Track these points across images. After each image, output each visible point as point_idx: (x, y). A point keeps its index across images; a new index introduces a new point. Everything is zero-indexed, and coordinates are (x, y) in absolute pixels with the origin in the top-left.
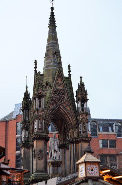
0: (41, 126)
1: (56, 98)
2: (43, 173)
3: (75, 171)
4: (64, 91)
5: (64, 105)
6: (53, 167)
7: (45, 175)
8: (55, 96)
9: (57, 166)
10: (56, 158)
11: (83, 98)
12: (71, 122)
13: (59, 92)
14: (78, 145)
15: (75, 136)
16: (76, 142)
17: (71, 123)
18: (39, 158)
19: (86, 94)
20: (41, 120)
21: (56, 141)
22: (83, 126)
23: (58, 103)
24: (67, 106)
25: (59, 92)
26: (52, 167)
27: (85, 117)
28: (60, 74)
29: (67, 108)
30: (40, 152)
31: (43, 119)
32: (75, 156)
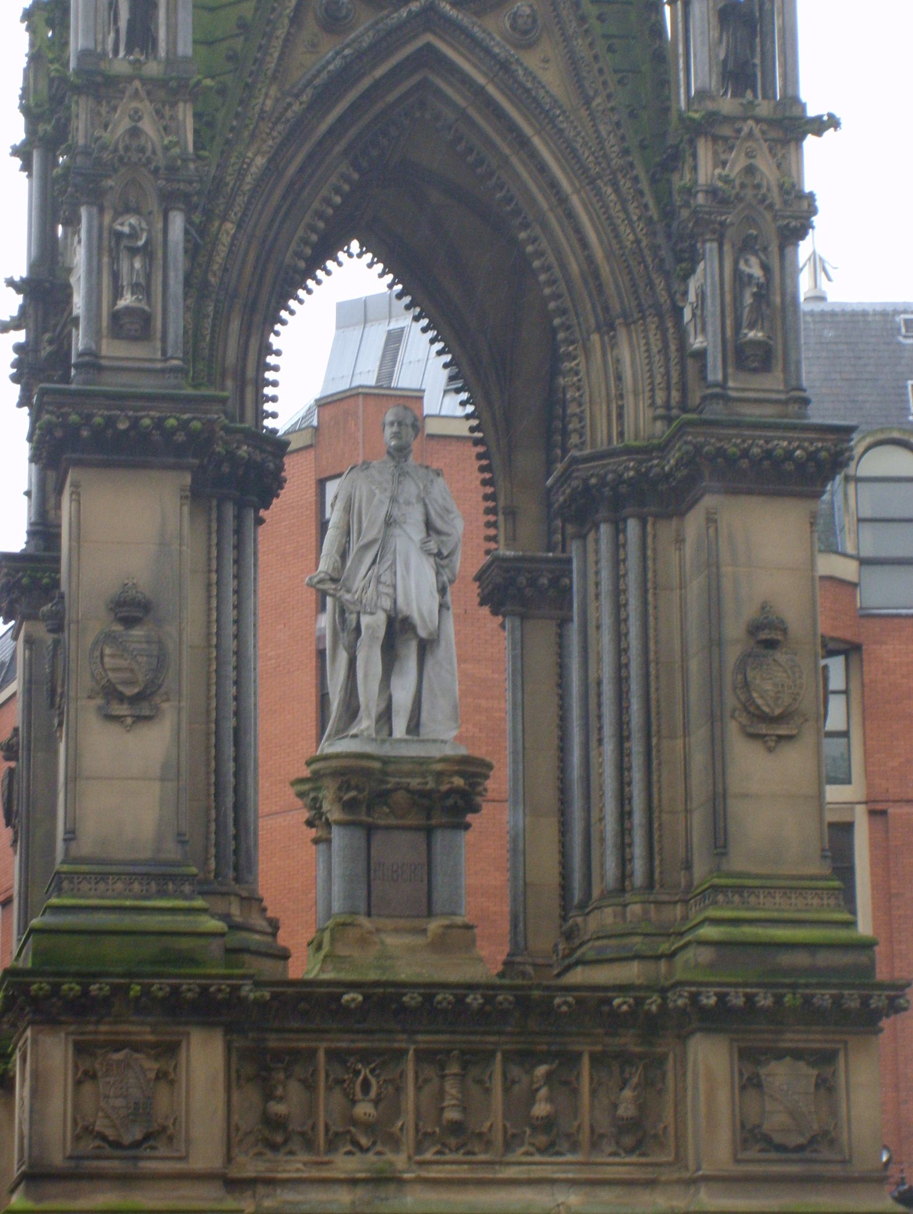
0: (143, 288)
2: (162, 894)
3: (639, 878)
6: (370, 830)
7: (181, 922)
10: (414, 726)
12: (584, 244)
14: (680, 541)
15: (641, 421)
16: (655, 490)
17: (590, 260)
18: (111, 693)
20: (153, 204)
21: (416, 515)
24: (525, 35)
26: (359, 835)
29: (531, 60)
30: (129, 622)
31: (169, 200)
32: (635, 686)
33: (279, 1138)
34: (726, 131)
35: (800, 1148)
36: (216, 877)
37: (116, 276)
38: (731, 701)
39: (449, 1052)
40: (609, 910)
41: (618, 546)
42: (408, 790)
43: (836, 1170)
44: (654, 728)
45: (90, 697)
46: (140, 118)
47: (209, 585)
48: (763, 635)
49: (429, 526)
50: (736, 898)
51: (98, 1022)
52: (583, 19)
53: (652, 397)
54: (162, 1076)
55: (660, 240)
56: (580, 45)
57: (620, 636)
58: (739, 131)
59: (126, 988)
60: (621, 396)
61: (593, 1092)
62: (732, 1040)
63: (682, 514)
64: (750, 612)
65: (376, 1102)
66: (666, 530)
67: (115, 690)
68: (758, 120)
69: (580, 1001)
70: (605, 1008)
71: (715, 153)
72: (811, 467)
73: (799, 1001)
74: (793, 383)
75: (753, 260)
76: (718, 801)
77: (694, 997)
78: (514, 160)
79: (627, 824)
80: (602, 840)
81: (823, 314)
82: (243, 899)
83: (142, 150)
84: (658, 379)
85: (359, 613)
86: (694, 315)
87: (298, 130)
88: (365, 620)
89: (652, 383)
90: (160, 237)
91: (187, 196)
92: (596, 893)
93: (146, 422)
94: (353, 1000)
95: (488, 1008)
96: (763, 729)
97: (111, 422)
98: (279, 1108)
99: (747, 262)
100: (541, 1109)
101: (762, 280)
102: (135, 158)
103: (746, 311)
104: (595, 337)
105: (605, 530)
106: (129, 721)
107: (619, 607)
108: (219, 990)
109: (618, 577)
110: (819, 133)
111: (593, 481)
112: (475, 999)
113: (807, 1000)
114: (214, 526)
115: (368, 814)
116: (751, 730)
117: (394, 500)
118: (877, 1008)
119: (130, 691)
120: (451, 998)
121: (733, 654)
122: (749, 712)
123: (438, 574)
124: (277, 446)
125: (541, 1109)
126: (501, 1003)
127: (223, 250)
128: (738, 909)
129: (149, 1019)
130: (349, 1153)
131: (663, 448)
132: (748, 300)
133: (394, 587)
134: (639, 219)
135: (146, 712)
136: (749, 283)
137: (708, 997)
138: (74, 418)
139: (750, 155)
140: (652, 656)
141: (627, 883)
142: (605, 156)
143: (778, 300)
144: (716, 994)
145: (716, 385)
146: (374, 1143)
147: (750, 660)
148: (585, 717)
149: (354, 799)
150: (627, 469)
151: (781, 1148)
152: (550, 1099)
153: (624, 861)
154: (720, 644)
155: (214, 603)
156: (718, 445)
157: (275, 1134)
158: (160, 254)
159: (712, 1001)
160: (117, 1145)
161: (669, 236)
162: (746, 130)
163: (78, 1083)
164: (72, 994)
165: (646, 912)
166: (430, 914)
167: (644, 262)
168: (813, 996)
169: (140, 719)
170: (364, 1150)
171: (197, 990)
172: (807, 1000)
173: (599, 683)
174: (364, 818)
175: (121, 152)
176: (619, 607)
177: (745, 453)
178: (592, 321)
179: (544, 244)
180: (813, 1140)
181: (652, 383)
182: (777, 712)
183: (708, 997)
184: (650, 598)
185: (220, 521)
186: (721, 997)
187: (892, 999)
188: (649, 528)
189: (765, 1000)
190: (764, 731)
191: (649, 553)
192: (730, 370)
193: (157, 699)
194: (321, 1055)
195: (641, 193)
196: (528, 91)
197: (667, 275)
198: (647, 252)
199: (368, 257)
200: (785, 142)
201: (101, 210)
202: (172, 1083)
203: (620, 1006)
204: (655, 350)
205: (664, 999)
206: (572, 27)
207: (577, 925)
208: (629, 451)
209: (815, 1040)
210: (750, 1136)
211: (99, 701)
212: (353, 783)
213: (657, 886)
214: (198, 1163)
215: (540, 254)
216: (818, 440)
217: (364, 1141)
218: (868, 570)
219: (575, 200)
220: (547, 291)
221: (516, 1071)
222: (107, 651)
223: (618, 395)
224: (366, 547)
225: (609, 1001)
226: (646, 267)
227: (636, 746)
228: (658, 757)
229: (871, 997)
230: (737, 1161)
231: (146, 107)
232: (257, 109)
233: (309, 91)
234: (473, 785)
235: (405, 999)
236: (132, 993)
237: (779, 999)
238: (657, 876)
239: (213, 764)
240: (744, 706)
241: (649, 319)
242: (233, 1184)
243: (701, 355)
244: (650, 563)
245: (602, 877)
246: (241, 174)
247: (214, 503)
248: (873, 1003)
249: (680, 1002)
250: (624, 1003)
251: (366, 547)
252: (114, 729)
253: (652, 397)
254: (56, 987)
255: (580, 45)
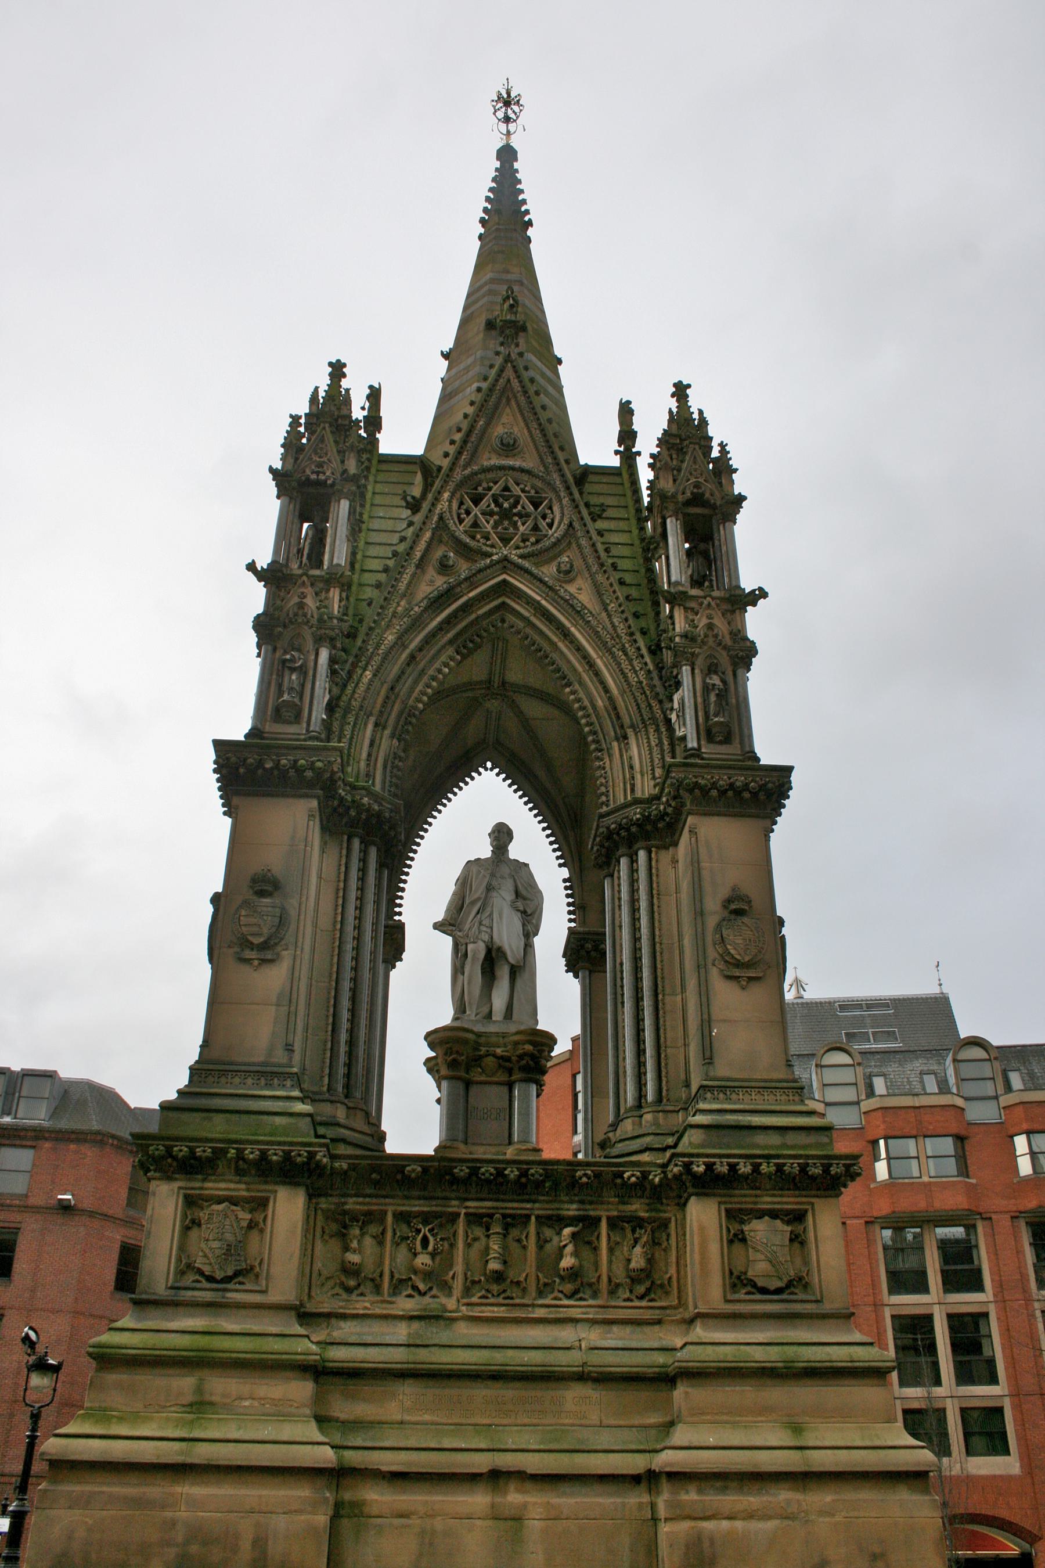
1: (475, 524)
2: (269, 1086)
3: (650, 1097)
4: (539, 484)
5: (549, 572)
6: (468, 1084)
8: (468, 513)
9: (502, 1077)
11: (697, 500)
12: (606, 690)
13: (506, 489)
14: (675, 861)
16: (657, 828)
17: (611, 699)
18: (245, 943)
19: (724, 469)
20: (310, 645)
21: (509, 885)
22: (707, 689)
23: (491, 555)
24: (567, 574)
25: (506, 489)
27: (719, 622)
28: (515, 384)
29: (572, 588)
30: (261, 893)
31: (319, 641)
32: (646, 961)
33: (352, 1283)
34: (693, 604)
35: (779, 1291)
36: (329, 1090)
37: (280, 686)
38: (712, 954)
39: (491, 1216)
40: (629, 1120)
41: (633, 871)
42: (494, 1056)
43: (810, 1308)
44: (660, 987)
45: (229, 947)
46: (305, 597)
47: (338, 889)
48: (733, 907)
49: (517, 894)
50: (721, 1096)
51: (204, 1180)
52: (602, 565)
53: (653, 774)
54: (252, 1225)
55: (656, 682)
56: (600, 578)
57: (635, 929)
58: (701, 604)
59: (225, 1151)
60: (633, 778)
61: (611, 1250)
62: (720, 1203)
63: (676, 844)
64: (724, 892)
65: (433, 1255)
66: (664, 857)
67: (248, 941)
68: (713, 598)
69: (597, 1175)
70: (619, 1181)
71: (686, 617)
72: (762, 796)
73: (773, 1169)
74: (747, 749)
75: (715, 677)
76: (706, 1023)
77: (687, 1166)
78: (560, 645)
79: (642, 1059)
80: (625, 1072)
81: (802, 1004)
82: (348, 1108)
83: (305, 615)
84: (656, 761)
85: (466, 944)
86: (678, 716)
87: (416, 624)
88: (470, 947)
89: (652, 765)
90: (312, 664)
91: (332, 639)
92: (622, 1111)
93: (284, 762)
94: (414, 1170)
95: (523, 1180)
96: (737, 972)
97: (260, 764)
98: (354, 1258)
99: (711, 679)
100: (567, 1262)
101: (722, 687)
102: (300, 620)
103: (712, 706)
104: (615, 744)
105: (624, 862)
106: (256, 962)
107: (634, 910)
108: (300, 1155)
109: (633, 891)
110: (754, 605)
111: (613, 826)
112: (512, 1172)
113: (780, 1168)
114: (344, 852)
115: (467, 1073)
116: (729, 974)
117: (493, 875)
118: (837, 1173)
119: (257, 940)
120: (492, 1170)
121: (712, 922)
122: (726, 961)
123: (524, 925)
124: (552, 1057)
125: (567, 1262)
126: (533, 1175)
127: (362, 687)
128: (722, 1103)
129: (246, 1179)
130: (410, 1296)
131: (658, 798)
132: (713, 698)
133: (492, 928)
134: (641, 669)
135: (269, 957)
136: (713, 689)
137: (698, 1166)
138: (233, 759)
139: (710, 617)
140: (657, 940)
141: (643, 1101)
142: (618, 636)
143: (734, 701)
144: (704, 1163)
145: (693, 749)
146: (431, 1289)
147: (725, 923)
148: (615, 994)
149: (454, 1060)
150: (635, 814)
151: (764, 1291)
152: (576, 1254)
153: (640, 1085)
154: (702, 914)
155: (340, 901)
156: (694, 780)
157: (352, 1278)
158: (311, 673)
159: (702, 1168)
160: (210, 1279)
161: (661, 678)
162: (706, 602)
163: (186, 1229)
164: (181, 1154)
165: (655, 1119)
166: (510, 1143)
167: (645, 693)
168: (784, 1164)
169: (264, 961)
170: (422, 1294)
171: (281, 1153)
172: (780, 1168)
173: (621, 964)
174: (462, 1074)
175: (291, 615)
176: (634, 910)
177: (714, 785)
178: (612, 733)
179: (582, 695)
180: (790, 1284)
181: (652, 765)
182: (747, 959)
183: (698, 1166)
184: (655, 901)
185: (349, 850)
186: (709, 1167)
187: (847, 1167)
188: (653, 855)
189: (745, 1168)
190: (738, 974)
191: (654, 871)
192: (703, 743)
193: (279, 948)
194: (390, 1218)
195: (642, 657)
196: (566, 601)
197: (661, 702)
198: (646, 688)
199: (497, 770)
200: (733, 612)
201: (275, 649)
202: (262, 1231)
203: (629, 1178)
204: (653, 744)
205: (664, 1172)
206: (595, 568)
207: (609, 1138)
208: (637, 802)
209: (788, 1201)
210: (738, 1281)
211: (237, 949)
212: (454, 1049)
213: (665, 1100)
214: (274, 1297)
215: (579, 700)
216: (766, 776)
217: (422, 1287)
218: (828, 1108)
219: (599, 662)
220: (587, 729)
221: (548, 1232)
222: (243, 913)
223: (631, 773)
224: (473, 903)
225: (620, 1175)
226: (646, 697)
227: (647, 1003)
228: (663, 1009)
229: (831, 1165)
230: (727, 1301)
231: (309, 591)
232: (391, 610)
233: (425, 602)
234: (541, 1051)
235: (456, 1171)
236: (229, 1155)
237: (756, 1168)
238: (664, 1093)
239: (332, 1010)
240: (721, 955)
241: (649, 727)
242: (305, 1317)
243: (684, 738)
244: (654, 878)
245: (626, 1100)
246: (377, 647)
247: (346, 837)
248: (833, 1170)
249: (676, 1170)
250: (633, 1175)
251: (473, 903)
252: (245, 969)
253: (653, 774)
254: (169, 1149)
255: (600, 578)
